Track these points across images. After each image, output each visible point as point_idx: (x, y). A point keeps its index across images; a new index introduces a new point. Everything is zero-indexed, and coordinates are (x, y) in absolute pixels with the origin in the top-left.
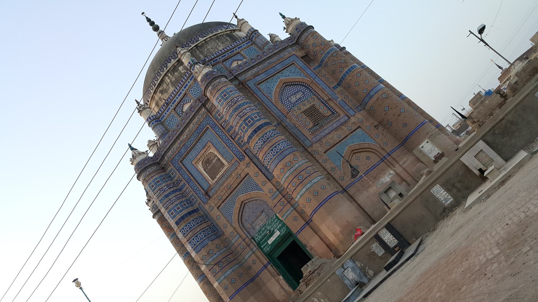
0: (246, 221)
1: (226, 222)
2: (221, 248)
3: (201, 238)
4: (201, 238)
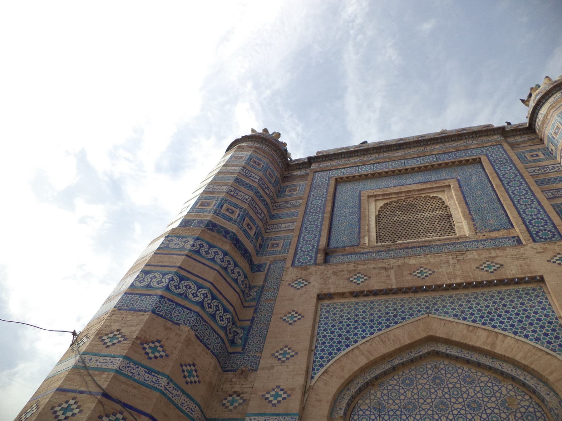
0: (380, 408)
1: (303, 344)
2: (189, 389)
3: (184, 296)
4: (184, 296)
